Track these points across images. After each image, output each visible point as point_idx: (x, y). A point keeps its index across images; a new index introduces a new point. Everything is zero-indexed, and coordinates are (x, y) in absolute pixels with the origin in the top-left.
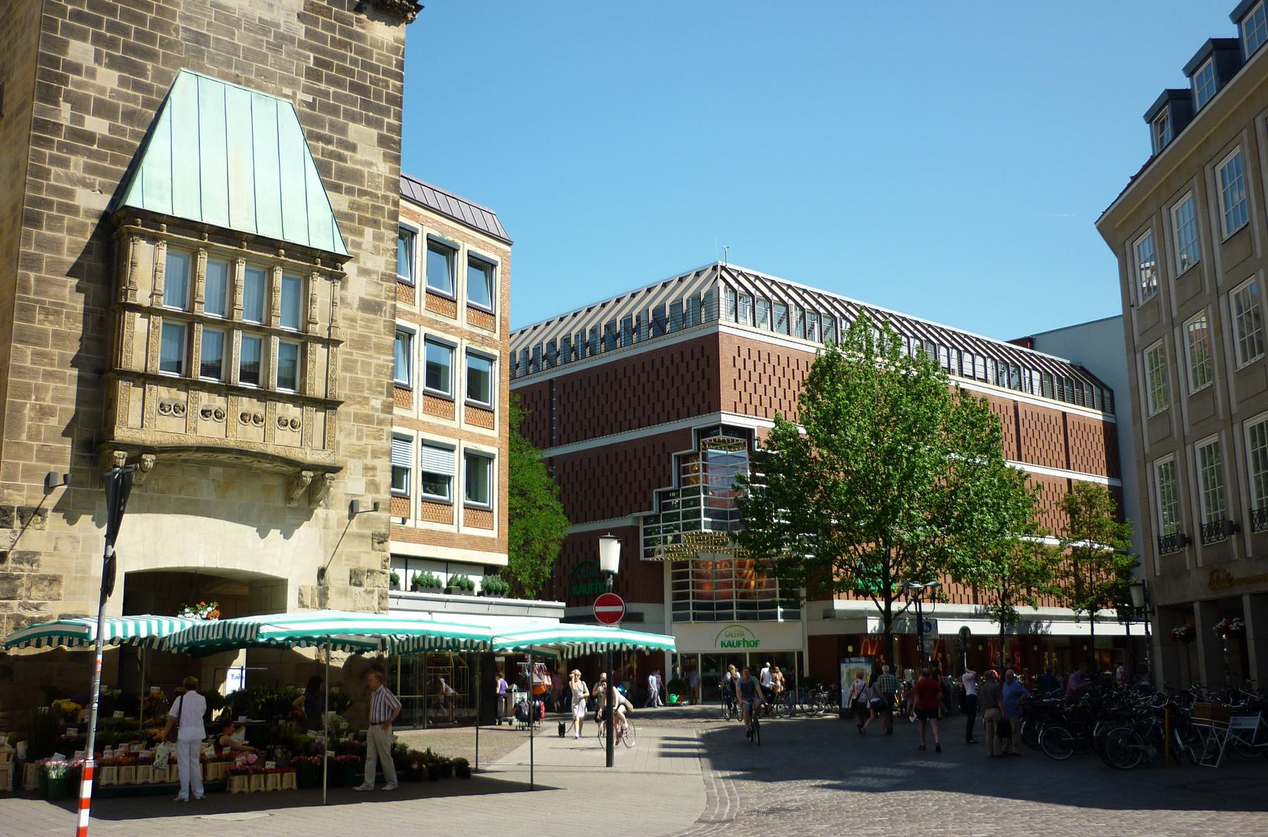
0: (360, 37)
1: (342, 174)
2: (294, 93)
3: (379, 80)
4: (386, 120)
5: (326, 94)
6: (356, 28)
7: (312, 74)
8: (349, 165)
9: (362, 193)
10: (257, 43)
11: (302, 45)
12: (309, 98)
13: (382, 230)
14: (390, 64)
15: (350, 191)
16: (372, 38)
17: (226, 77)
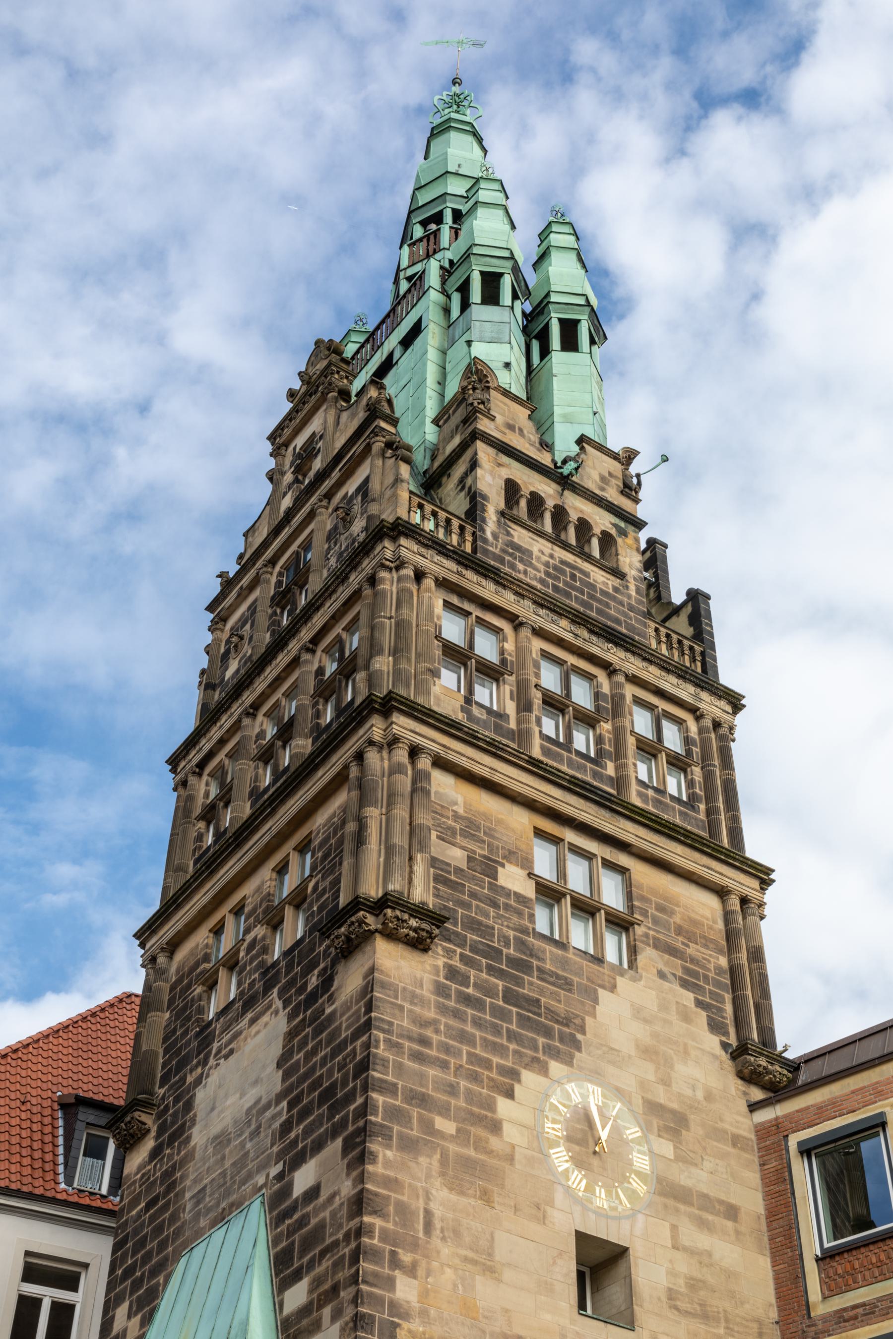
0: (332, 1017)
1: (307, 1244)
2: (268, 1175)
3: (348, 1055)
4: (352, 1107)
5: (295, 1142)
6: (328, 1011)
7: (286, 1128)
8: (314, 1221)
9: (323, 1254)
10: (243, 1145)
11: (279, 1098)
12: (279, 1167)
13: (342, 1294)
14: (359, 1018)
15: (311, 1265)
16: (341, 1006)
17: (214, 1224)
